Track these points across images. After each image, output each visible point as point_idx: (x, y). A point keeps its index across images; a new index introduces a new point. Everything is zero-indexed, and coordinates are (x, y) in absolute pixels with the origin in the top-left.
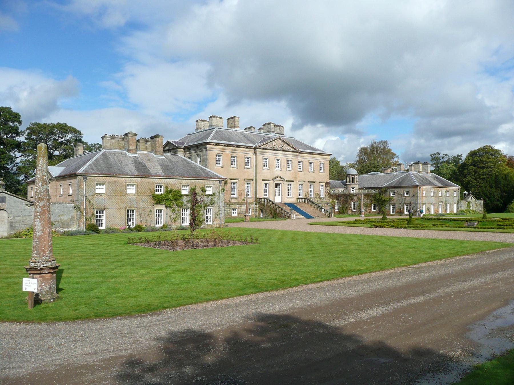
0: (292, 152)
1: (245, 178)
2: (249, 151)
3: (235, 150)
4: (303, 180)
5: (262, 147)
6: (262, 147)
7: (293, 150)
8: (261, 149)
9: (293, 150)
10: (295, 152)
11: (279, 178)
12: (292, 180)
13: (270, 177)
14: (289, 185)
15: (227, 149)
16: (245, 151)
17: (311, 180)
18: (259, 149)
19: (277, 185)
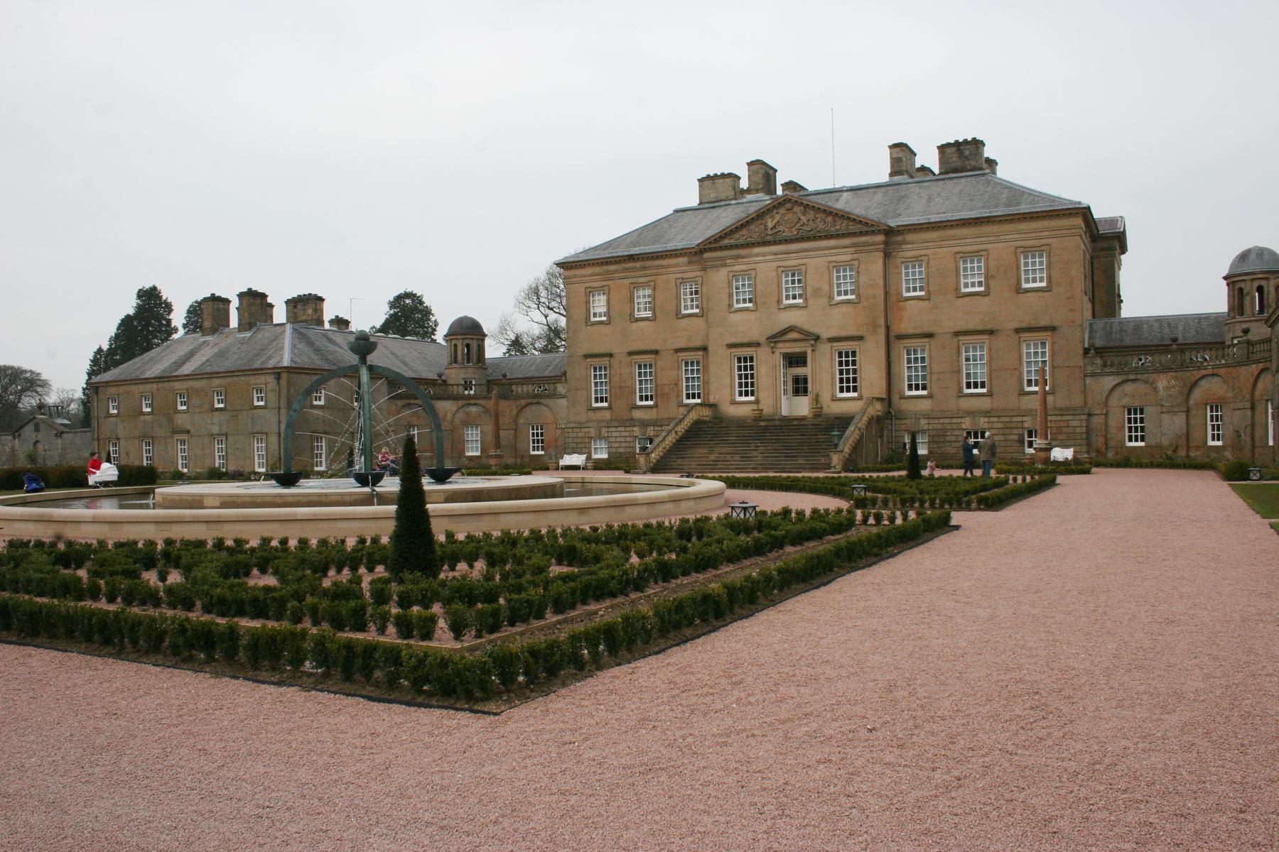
0: (854, 234)
1: (682, 344)
2: (690, 263)
3: (644, 268)
4: (927, 330)
5: (726, 242)
6: (726, 242)
7: (858, 228)
8: (715, 249)
9: (858, 228)
10: (861, 234)
11: (794, 335)
12: (856, 333)
13: (756, 334)
14: (795, 360)
15: (616, 271)
16: (677, 265)
17: (970, 327)
18: (711, 250)
19: (795, 360)
